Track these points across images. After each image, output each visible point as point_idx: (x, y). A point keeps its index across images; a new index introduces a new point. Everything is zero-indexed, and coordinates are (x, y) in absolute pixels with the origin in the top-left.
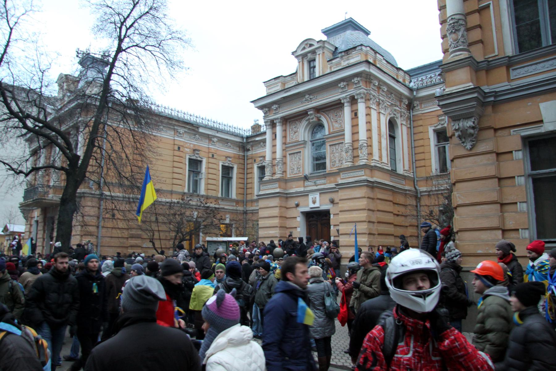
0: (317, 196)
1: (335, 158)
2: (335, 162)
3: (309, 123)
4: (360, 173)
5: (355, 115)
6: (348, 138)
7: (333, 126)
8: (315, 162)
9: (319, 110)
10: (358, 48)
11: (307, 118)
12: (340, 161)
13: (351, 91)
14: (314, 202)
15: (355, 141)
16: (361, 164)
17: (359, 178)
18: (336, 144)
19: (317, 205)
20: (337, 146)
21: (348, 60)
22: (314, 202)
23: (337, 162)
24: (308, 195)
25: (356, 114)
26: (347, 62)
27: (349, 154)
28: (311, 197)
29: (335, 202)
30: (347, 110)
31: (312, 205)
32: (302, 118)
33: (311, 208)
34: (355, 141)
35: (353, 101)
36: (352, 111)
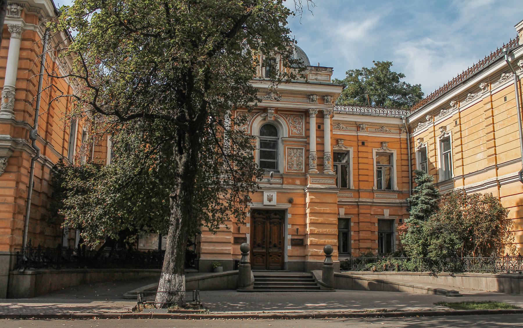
0: (274, 195)
1: (293, 161)
2: (293, 165)
3: (264, 119)
4: (329, 181)
5: (320, 127)
6: (313, 147)
7: (292, 131)
8: (275, 161)
9: (277, 110)
10: (328, 70)
11: (263, 115)
12: (297, 165)
13: (321, 107)
14: (270, 200)
15: (321, 151)
16: (330, 173)
17: (330, 185)
18: (294, 149)
19: (272, 203)
20: (295, 150)
21: (316, 74)
22: (270, 200)
23: (295, 166)
24: (263, 192)
25: (319, 127)
26: (314, 77)
27: (316, 162)
28: (266, 194)
29: (294, 203)
30: (313, 122)
31: (266, 202)
32: (258, 113)
33: (265, 205)
34: (321, 151)
35: (321, 115)
36: (317, 123)
